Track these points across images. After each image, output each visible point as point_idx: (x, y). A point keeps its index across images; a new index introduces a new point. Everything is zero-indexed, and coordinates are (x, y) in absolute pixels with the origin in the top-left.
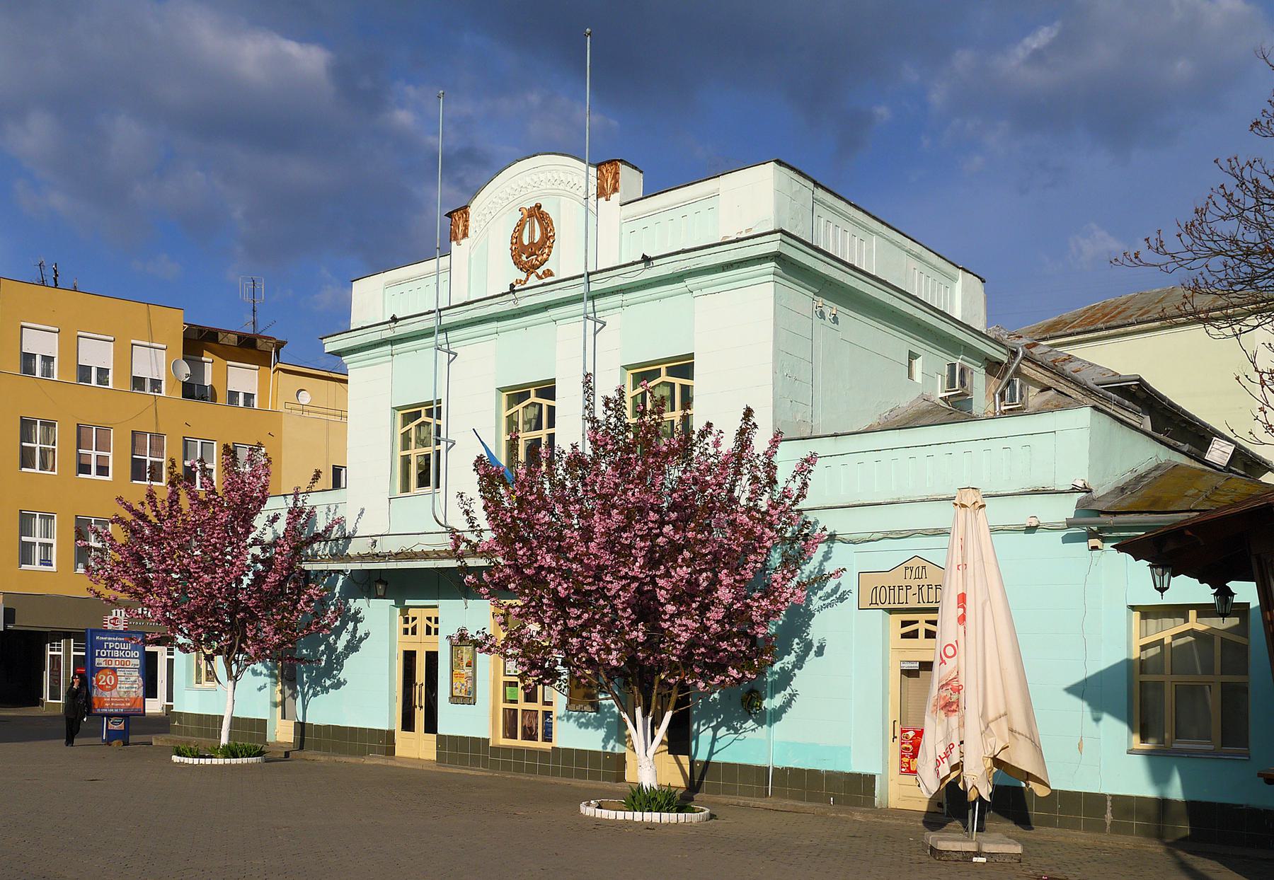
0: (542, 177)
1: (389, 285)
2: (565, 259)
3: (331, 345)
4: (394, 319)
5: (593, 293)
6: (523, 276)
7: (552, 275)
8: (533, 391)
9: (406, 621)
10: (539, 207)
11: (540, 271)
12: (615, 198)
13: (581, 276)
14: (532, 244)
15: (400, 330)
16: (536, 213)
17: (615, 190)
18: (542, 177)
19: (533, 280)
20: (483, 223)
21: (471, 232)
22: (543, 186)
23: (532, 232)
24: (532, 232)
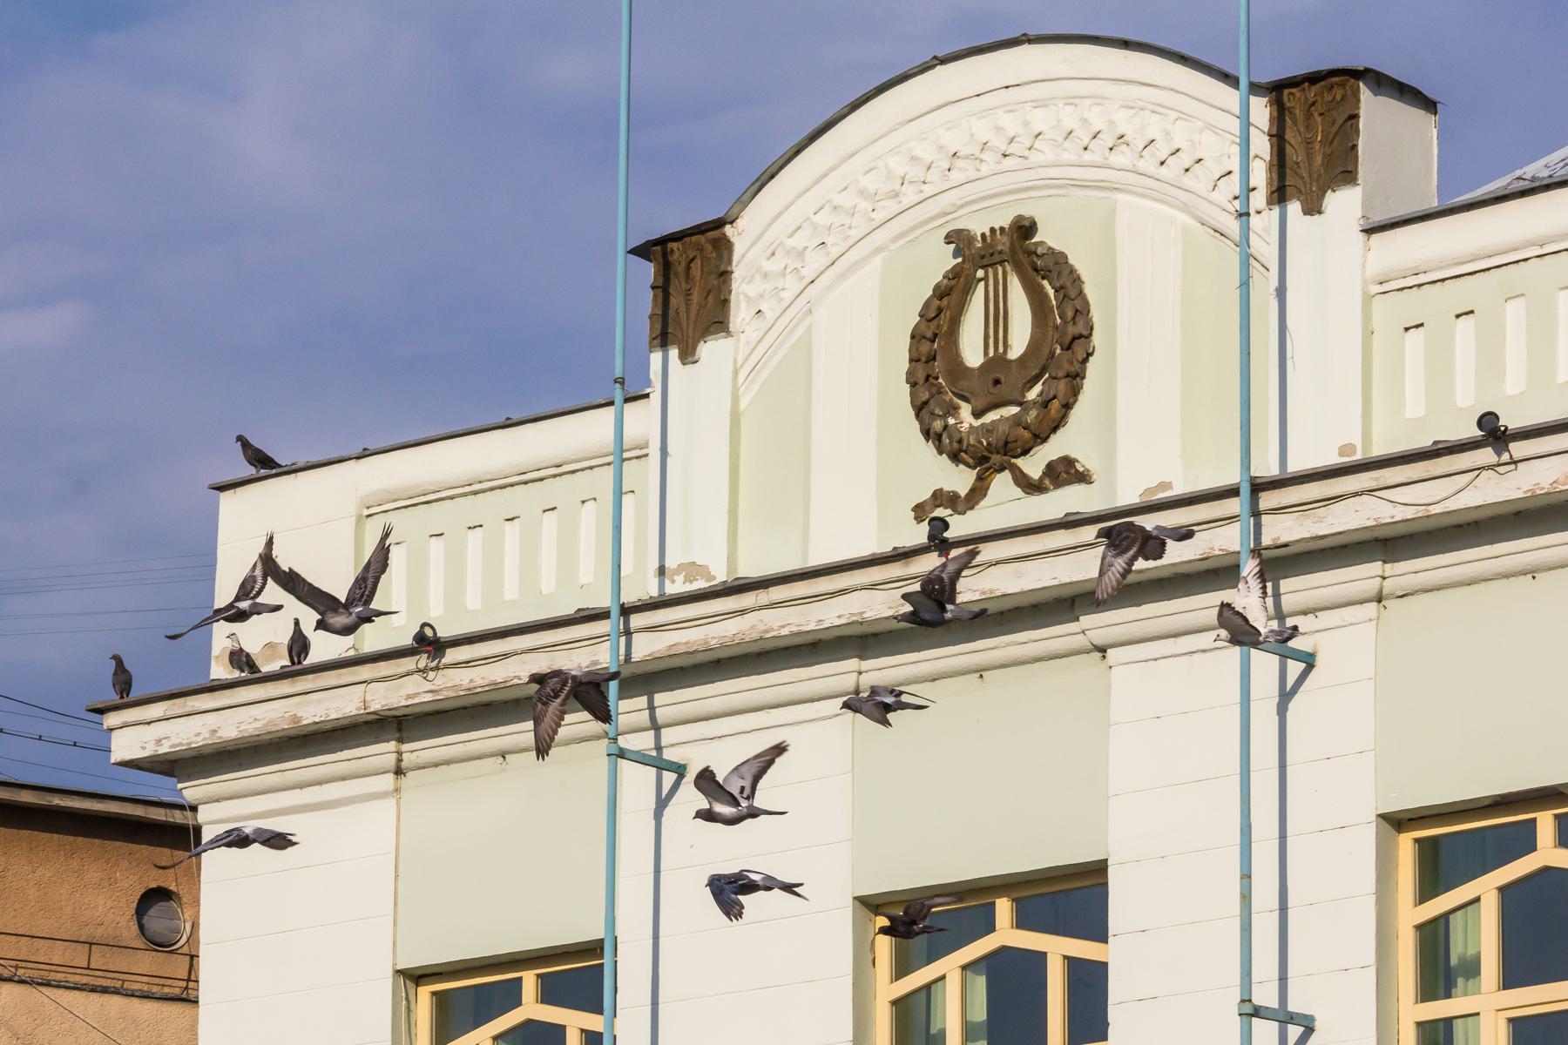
0: (1040, 120)
2: (1142, 431)
6: (961, 479)
7: (1083, 478)
10: (1024, 229)
11: (1033, 466)
12: (1344, 204)
13: (1233, 492)
14: (996, 363)
16: (1018, 250)
17: (1348, 176)
18: (1040, 120)
19: (1004, 504)
20: (792, 285)
21: (740, 314)
22: (1045, 153)
23: (997, 319)
24: (997, 319)
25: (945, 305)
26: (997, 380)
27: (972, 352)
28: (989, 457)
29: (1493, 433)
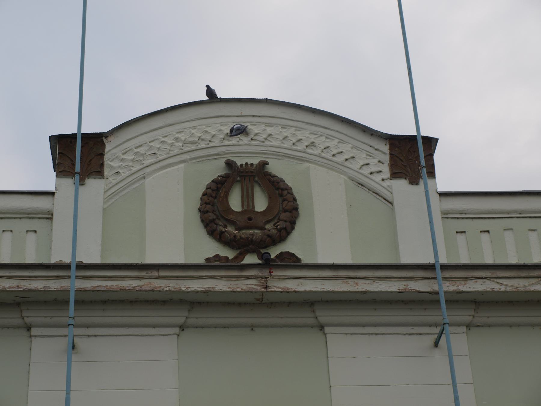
26: (249, 216)
27: (235, 202)
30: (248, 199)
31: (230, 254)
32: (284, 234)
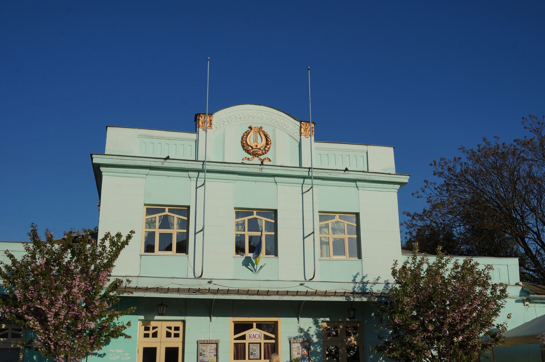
1: (140, 136)
3: (97, 159)
4: (168, 158)
5: (308, 176)
8: (255, 212)
9: (147, 329)
10: (261, 128)
11: (262, 157)
15: (167, 164)
25: (247, 134)
28: (255, 154)
29: (346, 170)
30: (256, 140)
31: (250, 157)
32: (266, 152)
